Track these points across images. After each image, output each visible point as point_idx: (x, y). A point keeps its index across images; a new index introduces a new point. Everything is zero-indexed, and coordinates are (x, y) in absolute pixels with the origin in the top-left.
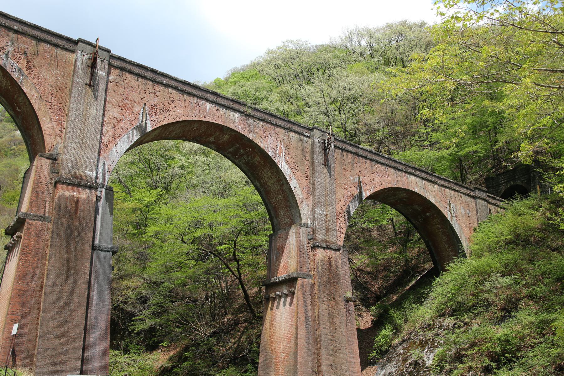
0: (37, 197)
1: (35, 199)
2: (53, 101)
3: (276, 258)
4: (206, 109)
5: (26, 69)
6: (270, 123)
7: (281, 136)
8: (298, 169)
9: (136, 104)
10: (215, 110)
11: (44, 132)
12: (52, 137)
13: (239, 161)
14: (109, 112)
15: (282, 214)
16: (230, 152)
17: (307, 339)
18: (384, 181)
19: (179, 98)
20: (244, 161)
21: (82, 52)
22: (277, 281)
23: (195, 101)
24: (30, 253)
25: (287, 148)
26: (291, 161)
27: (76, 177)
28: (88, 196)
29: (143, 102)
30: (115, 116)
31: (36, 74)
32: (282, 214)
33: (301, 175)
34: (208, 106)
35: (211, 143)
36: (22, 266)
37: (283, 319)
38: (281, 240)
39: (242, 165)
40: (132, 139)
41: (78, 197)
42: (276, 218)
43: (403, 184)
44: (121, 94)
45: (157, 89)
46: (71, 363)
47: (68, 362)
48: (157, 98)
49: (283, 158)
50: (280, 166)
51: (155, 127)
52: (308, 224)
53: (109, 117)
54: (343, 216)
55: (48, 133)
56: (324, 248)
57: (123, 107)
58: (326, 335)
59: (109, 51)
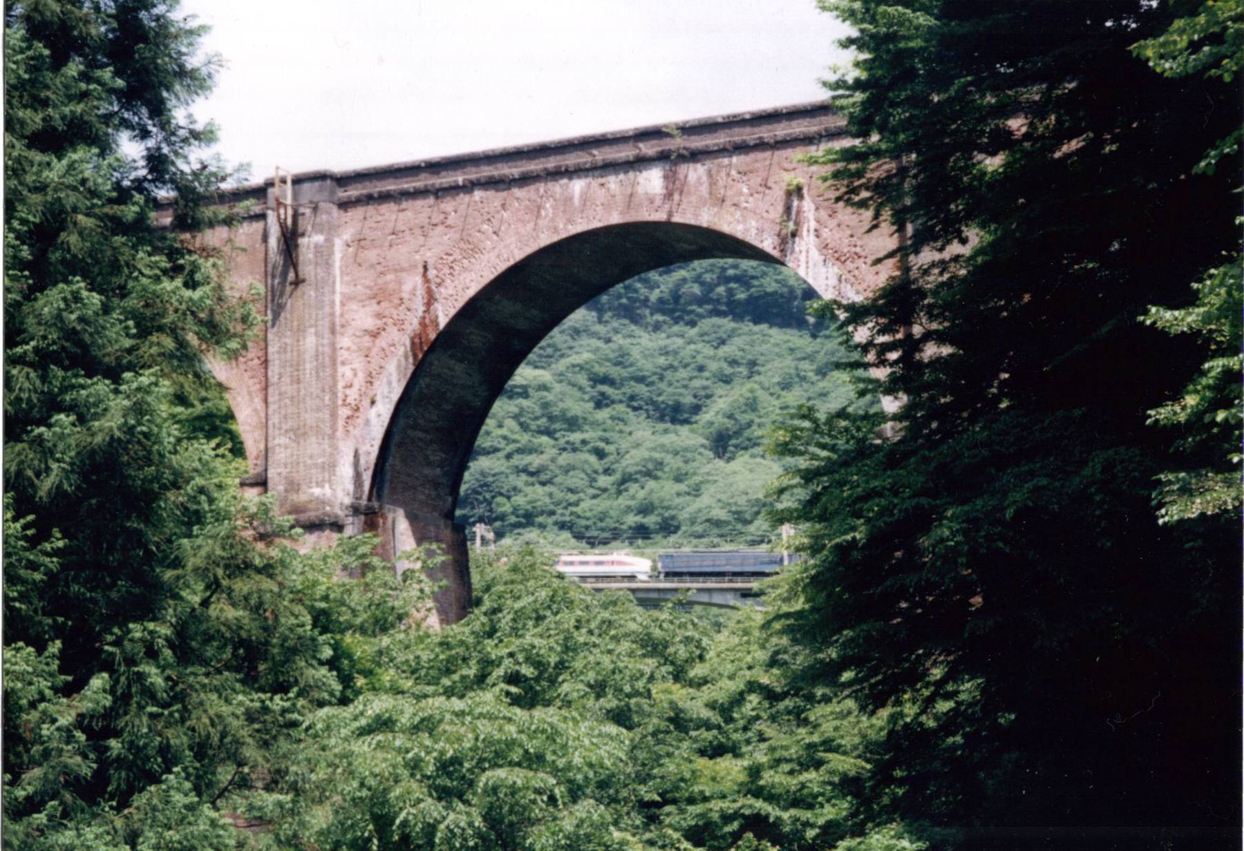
4: (570, 199)
6: (761, 146)
34: (577, 186)
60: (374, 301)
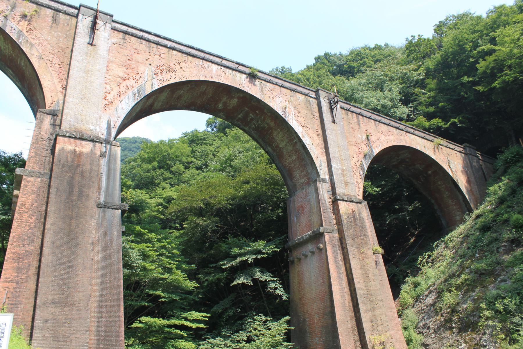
0: (36, 153)
1: (34, 155)
2: (54, 60)
3: (297, 219)
5: (26, 30)
6: (277, 84)
7: (289, 97)
8: (309, 127)
9: (140, 64)
10: (222, 72)
11: (44, 89)
12: (53, 94)
13: (250, 128)
14: (113, 71)
15: (298, 175)
16: (240, 119)
17: (342, 296)
18: (389, 139)
19: (185, 61)
20: (254, 126)
21: (83, 15)
22: (301, 240)
23: (201, 63)
24: (27, 212)
25: (295, 107)
26: (301, 120)
27: (78, 131)
28: (92, 150)
29: (148, 63)
30: (120, 75)
31: (37, 35)
32: (298, 175)
33: (313, 133)
34: (214, 67)
35: (220, 111)
36: (18, 226)
37: (313, 278)
38: (300, 200)
39: (253, 132)
40: (138, 96)
41: (80, 151)
42: (291, 181)
43: (406, 143)
44: (125, 55)
45: (162, 52)
46: (77, 336)
47: (73, 336)
48: (162, 59)
49: (293, 116)
50: (291, 125)
51: (161, 86)
52: (326, 179)
53: (113, 75)
54: (358, 172)
55: (48, 89)
56: (346, 201)
57: (127, 67)
58: (362, 289)
59: (112, 16)
60: (125, 68)
